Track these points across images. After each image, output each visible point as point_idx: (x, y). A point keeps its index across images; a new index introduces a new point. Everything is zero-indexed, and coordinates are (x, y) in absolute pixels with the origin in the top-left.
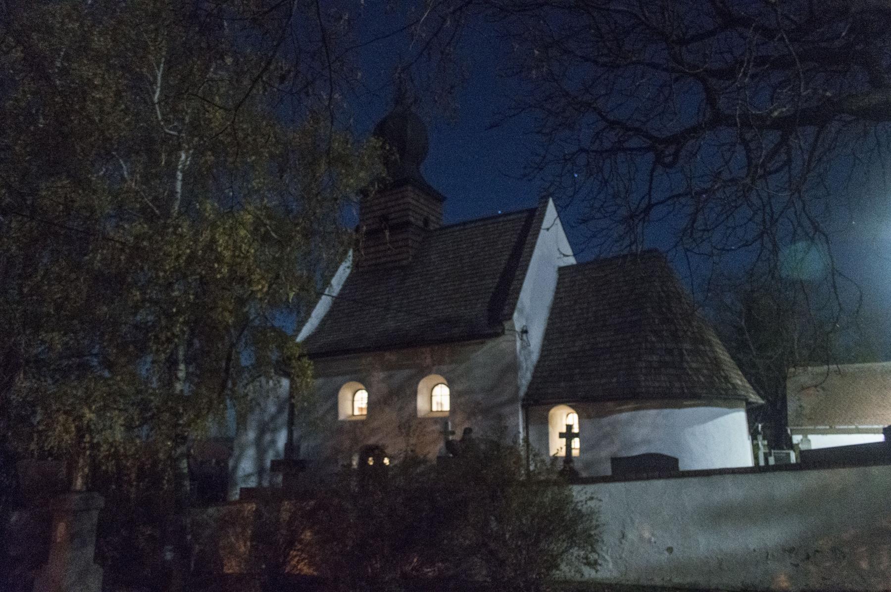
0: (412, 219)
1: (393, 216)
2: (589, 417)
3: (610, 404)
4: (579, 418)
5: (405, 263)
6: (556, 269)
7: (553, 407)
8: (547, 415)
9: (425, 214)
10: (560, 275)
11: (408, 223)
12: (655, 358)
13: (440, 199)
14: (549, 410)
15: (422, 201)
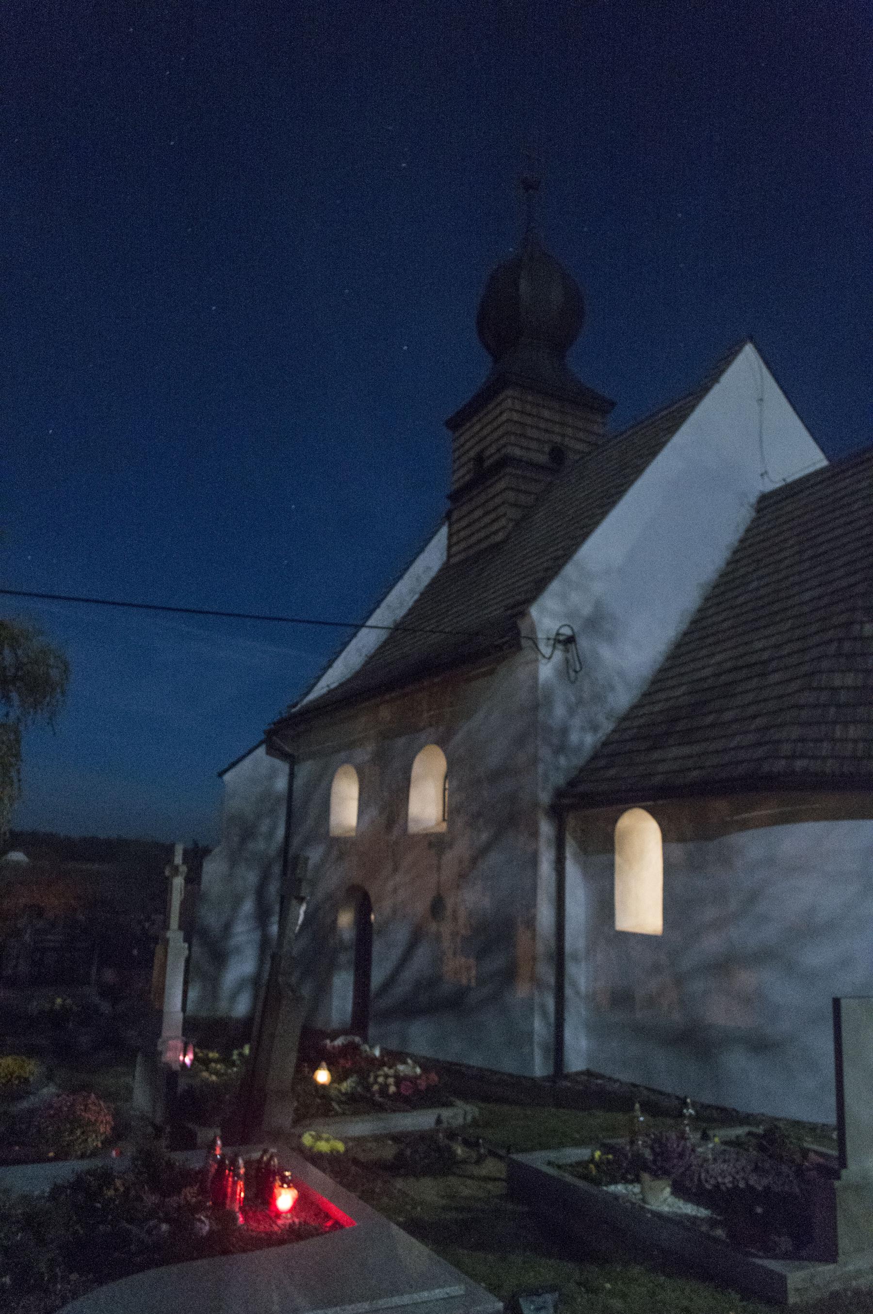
0: (518, 452)
1: (487, 453)
2: (682, 839)
3: (721, 806)
4: (666, 839)
5: (500, 536)
6: (753, 499)
7: (625, 810)
8: (613, 830)
9: (558, 439)
10: (758, 511)
11: (505, 462)
12: (850, 680)
13: (604, 406)
14: (615, 821)
15: (546, 413)
